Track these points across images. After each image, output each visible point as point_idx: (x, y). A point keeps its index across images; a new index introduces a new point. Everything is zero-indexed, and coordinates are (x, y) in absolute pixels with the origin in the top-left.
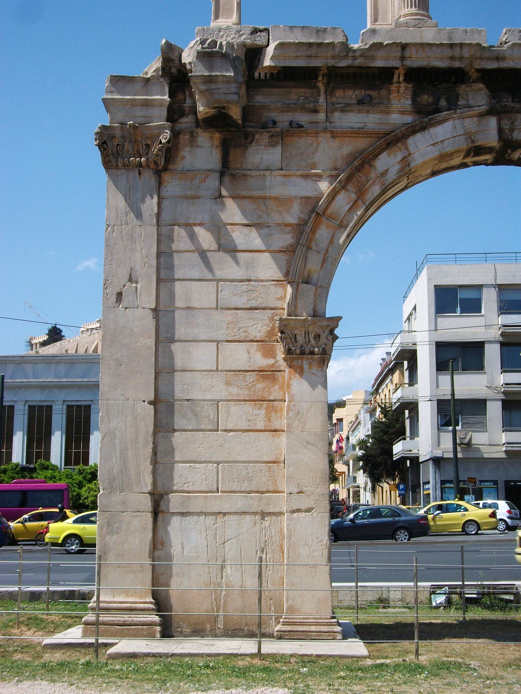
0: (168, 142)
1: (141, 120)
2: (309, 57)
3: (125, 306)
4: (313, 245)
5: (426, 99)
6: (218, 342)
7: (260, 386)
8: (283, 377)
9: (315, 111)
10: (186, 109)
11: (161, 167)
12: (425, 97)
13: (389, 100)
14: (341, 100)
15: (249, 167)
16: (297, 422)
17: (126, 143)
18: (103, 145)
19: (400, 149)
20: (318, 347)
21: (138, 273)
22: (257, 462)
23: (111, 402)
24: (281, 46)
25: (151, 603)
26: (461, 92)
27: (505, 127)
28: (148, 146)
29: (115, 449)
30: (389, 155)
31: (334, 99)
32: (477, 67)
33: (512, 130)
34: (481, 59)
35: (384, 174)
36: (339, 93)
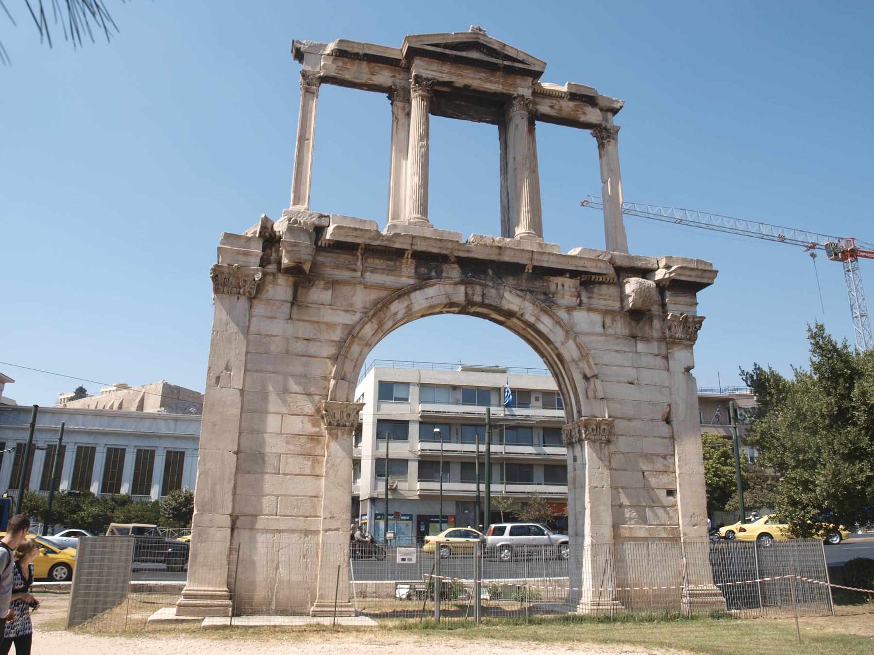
0: (260, 280)
1: (242, 264)
2: (356, 237)
3: (222, 385)
4: (348, 355)
5: (423, 270)
6: (283, 415)
7: (309, 445)
8: (325, 440)
9: (355, 270)
10: (272, 260)
11: (253, 296)
12: (423, 269)
13: (401, 269)
14: (371, 266)
15: (310, 302)
16: (332, 471)
17: (231, 278)
18: (215, 278)
19: (406, 300)
20: (348, 422)
21: (232, 365)
22: (304, 496)
23: (207, 451)
24: (338, 228)
25: (225, 591)
26: (444, 268)
27: (469, 292)
28: (245, 281)
29: (208, 483)
30: (399, 302)
31: (367, 264)
32: (456, 255)
33: (473, 295)
34: (459, 250)
35: (395, 314)
36: (370, 261)
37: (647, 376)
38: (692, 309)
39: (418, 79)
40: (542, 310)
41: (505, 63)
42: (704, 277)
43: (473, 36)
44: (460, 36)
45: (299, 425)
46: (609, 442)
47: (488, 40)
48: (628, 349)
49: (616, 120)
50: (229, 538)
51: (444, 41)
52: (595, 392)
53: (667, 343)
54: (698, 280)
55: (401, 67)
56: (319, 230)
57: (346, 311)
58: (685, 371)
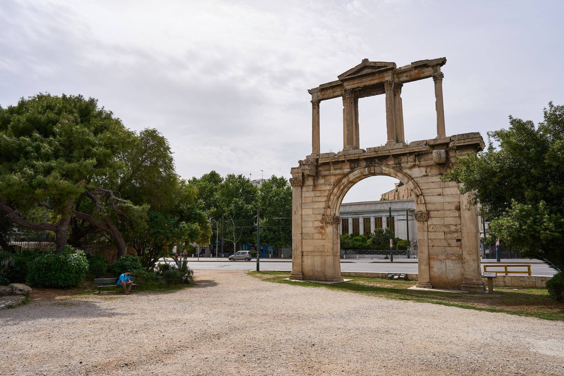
5: (353, 165)
7: (320, 230)
33: (371, 171)
37: (448, 191)
39: (345, 90)
40: (398, 171)
43: (363, 64)
44: (358, 67)
45: (318, 224)
46: (427, 221)
47: (369, 63)
49: (443, 69)
51: (352, 72)
52: (421, 201)
54: (470, 143)
56: (317, 160)
57: (329, 185)
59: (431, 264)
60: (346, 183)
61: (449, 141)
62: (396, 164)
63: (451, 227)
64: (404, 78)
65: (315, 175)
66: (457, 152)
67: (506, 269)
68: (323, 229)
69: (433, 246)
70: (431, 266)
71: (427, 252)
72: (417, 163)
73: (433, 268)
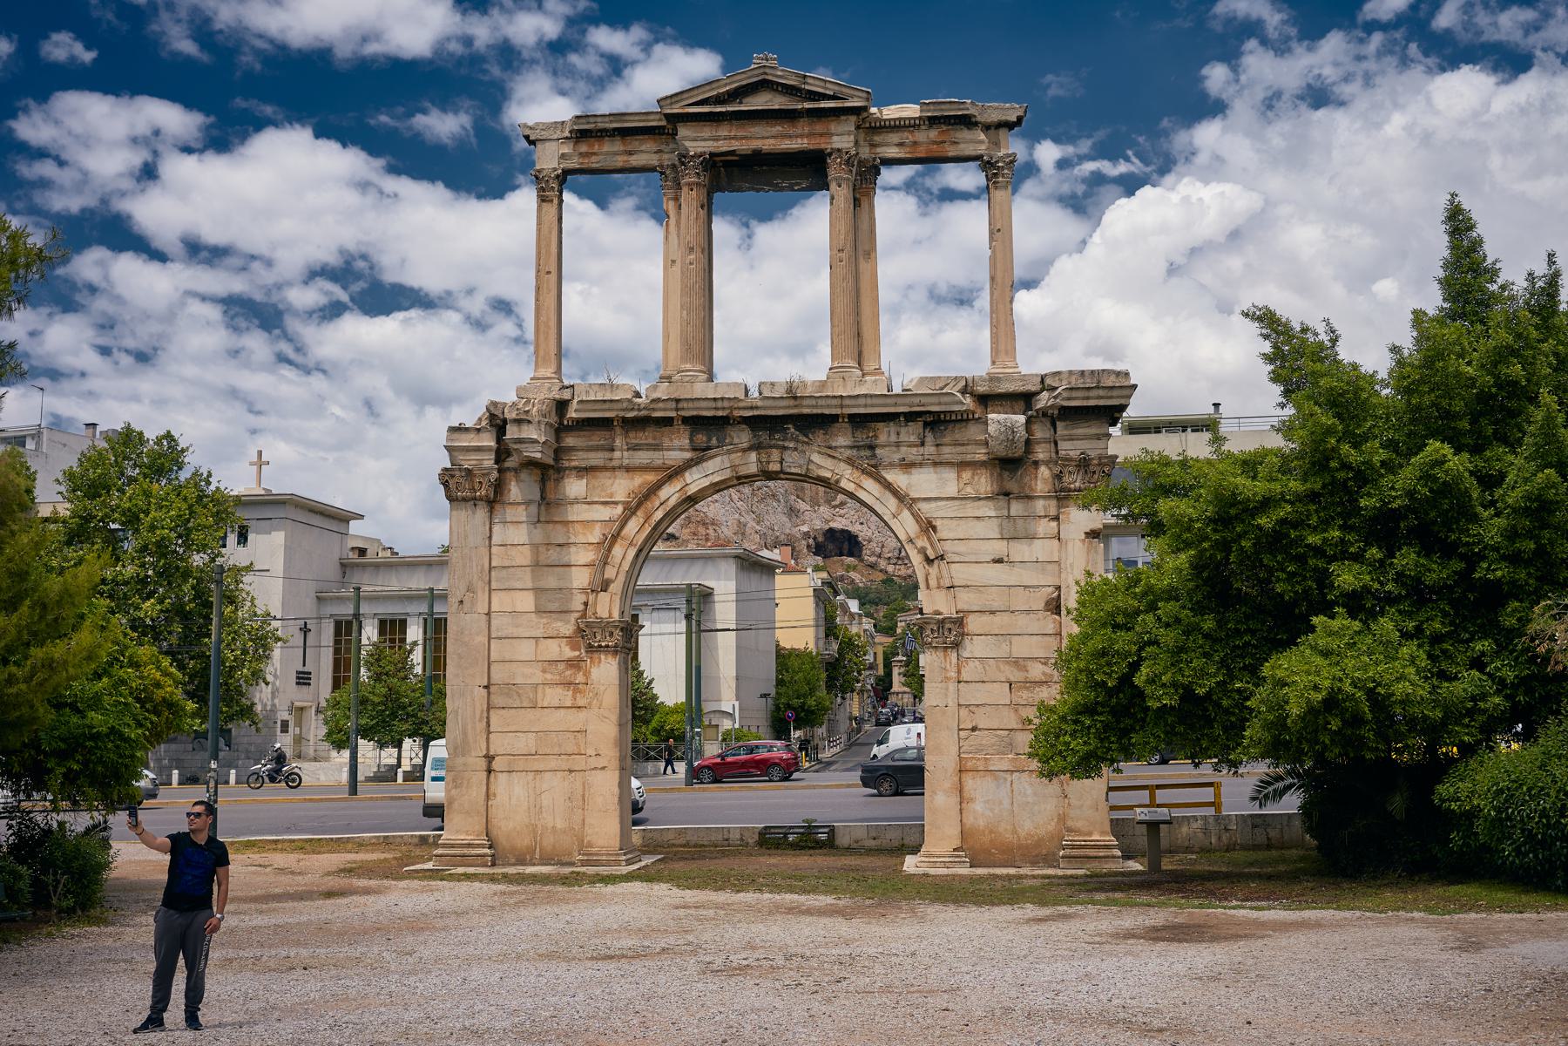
5: (701, 438)
6: (537, 639)
7: (568, 673)
9: (613, 450)
14: (633, 441)
18: (445, 484)
28: (480, 482)
31: (628, 440)
33: (768, 463)
36: (632, 434)
37: (1021, 551)
38: (1101, 444)
39: (683, 156)
40: (864, 471)
41: (807, 105)
42: (1111, 397)
45: (559, 650)
46: (956, 645)
48: (993, 514)
50: (485, 782)
53: (1058, 499)
54: (1102, 403)
55: (668, 134)
56: (562, 406)
57: (605, 503)
58: (1087, 537)
59: (966, 789)
60: (672, 502)
61: (1038, 387)
62: (858, 448)
63: (1029, 668)
64: (892, 152)
65: (552, 462)
66: (1060, 425)
67: (1152, 796)
68: (579, 668)
69: (974, 729)
70: (966, 795)
71: (954, 750)
72: (929, 449)
73: (971, 800)
